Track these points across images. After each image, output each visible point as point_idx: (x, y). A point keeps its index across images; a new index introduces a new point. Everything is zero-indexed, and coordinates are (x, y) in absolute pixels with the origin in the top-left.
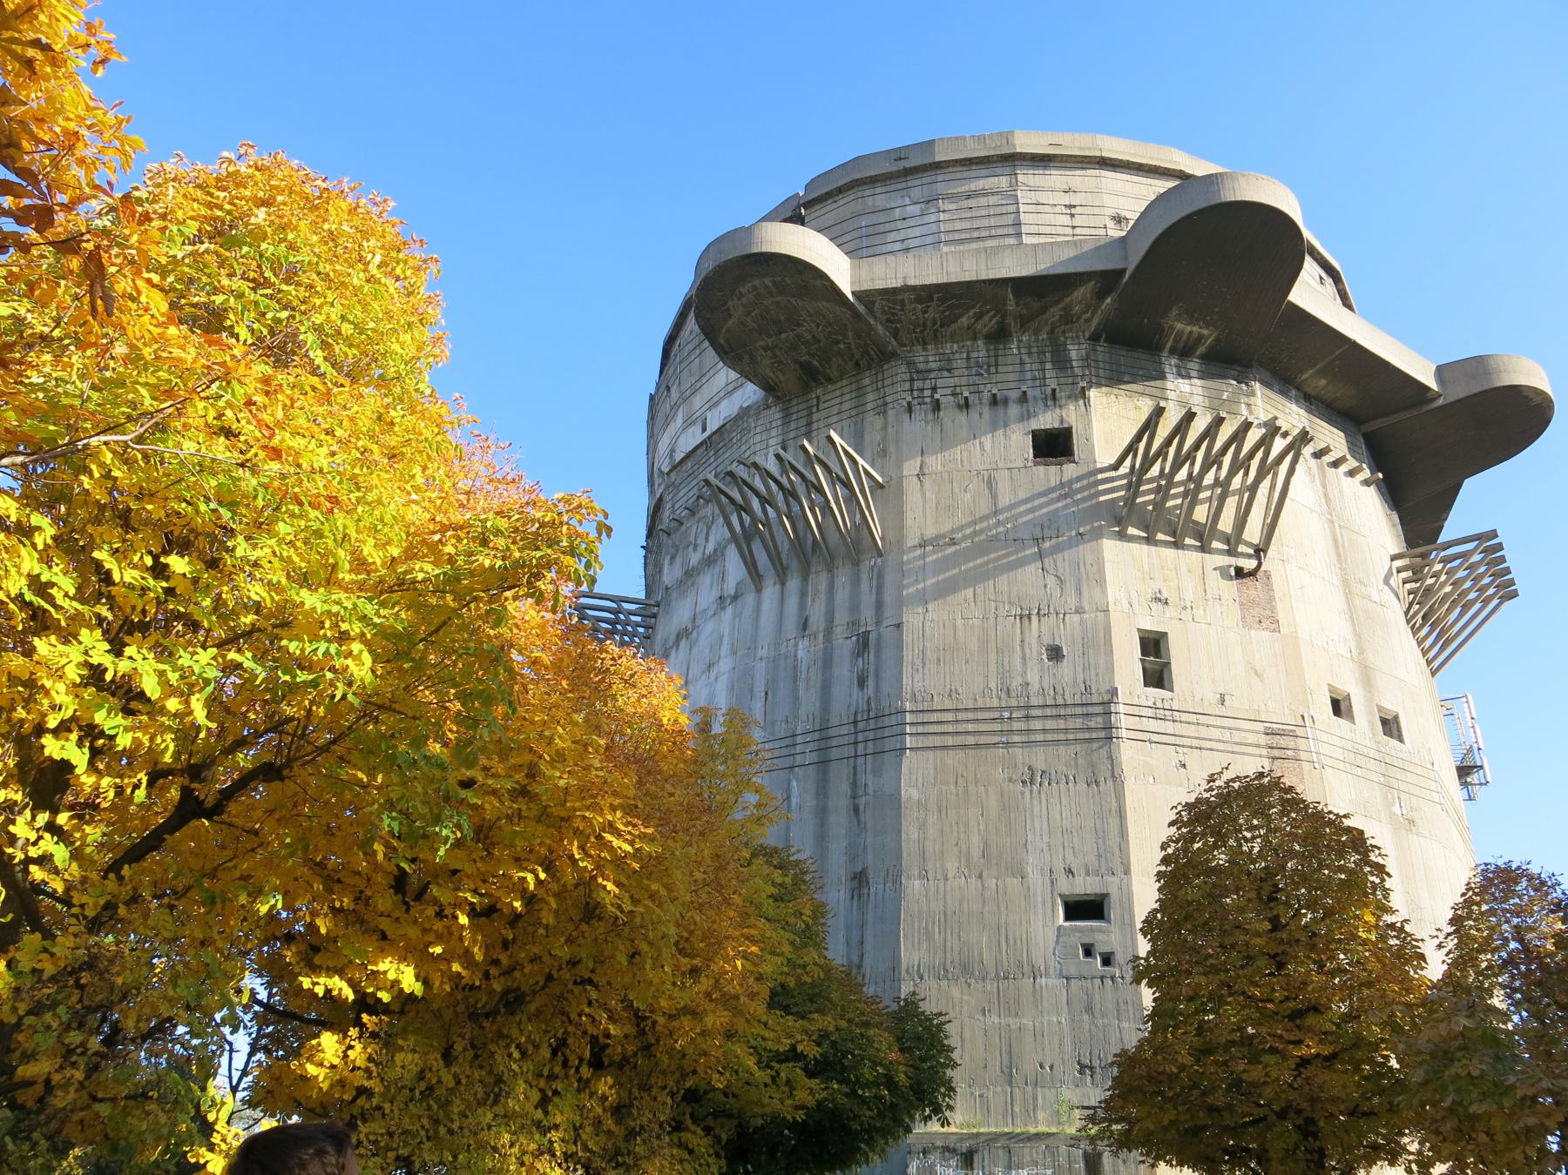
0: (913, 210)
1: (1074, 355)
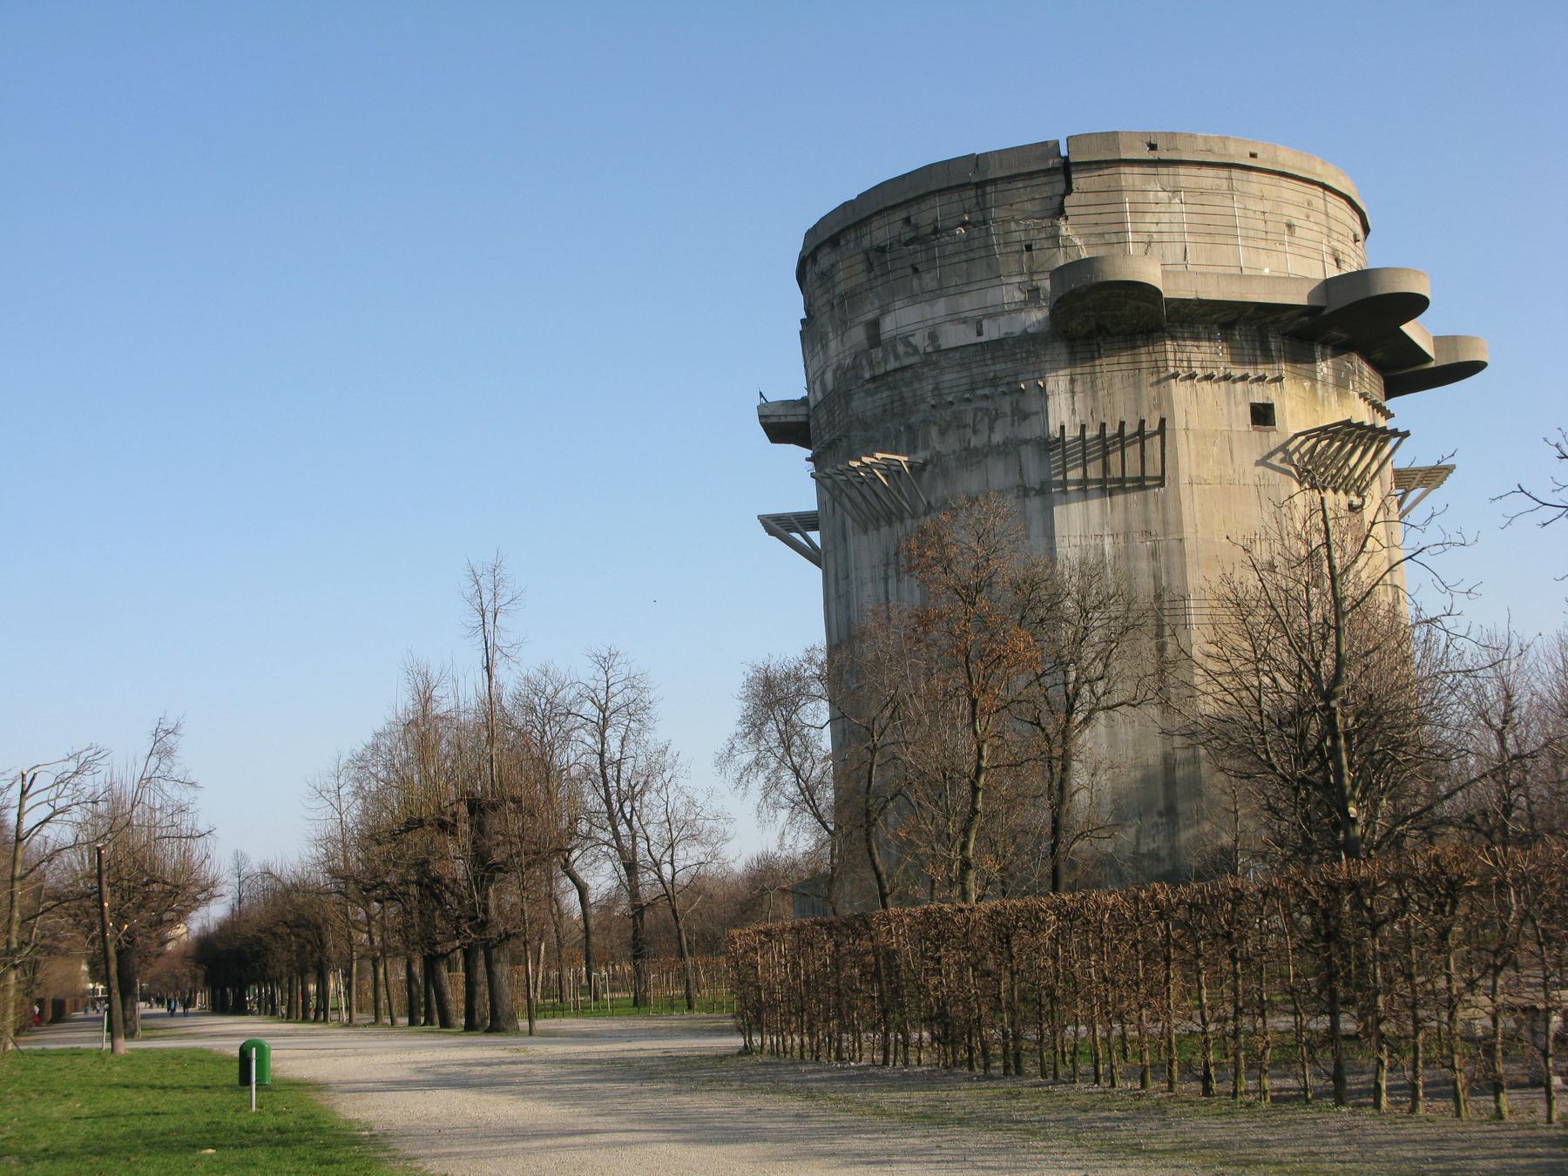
0: (1163, 195)
1: (1273, 347)
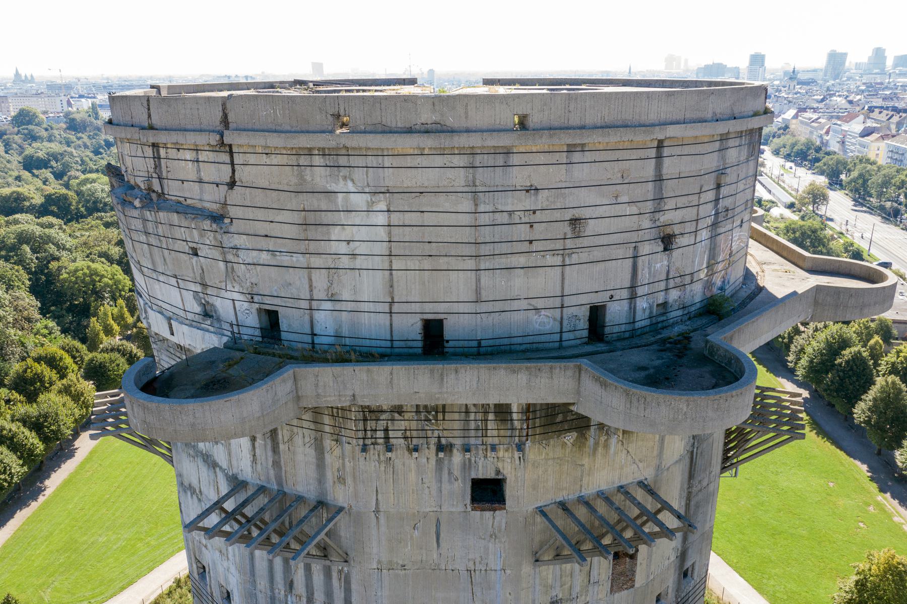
0: (360, 201)
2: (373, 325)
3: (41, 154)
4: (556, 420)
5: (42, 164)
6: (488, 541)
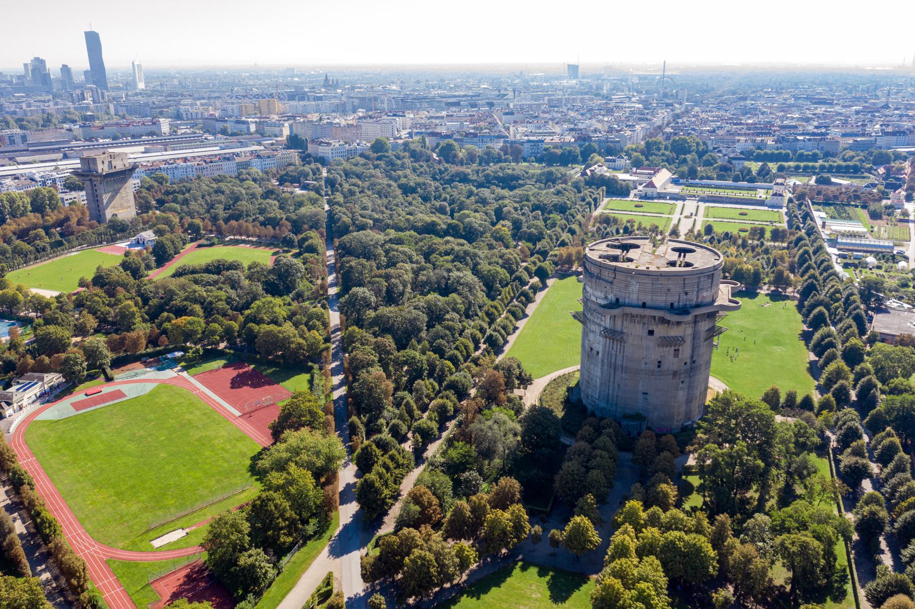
2: (635, 302)
3: (412, 184)
4: (663, 321)
5: (413, 190)
6: (650, 342)
